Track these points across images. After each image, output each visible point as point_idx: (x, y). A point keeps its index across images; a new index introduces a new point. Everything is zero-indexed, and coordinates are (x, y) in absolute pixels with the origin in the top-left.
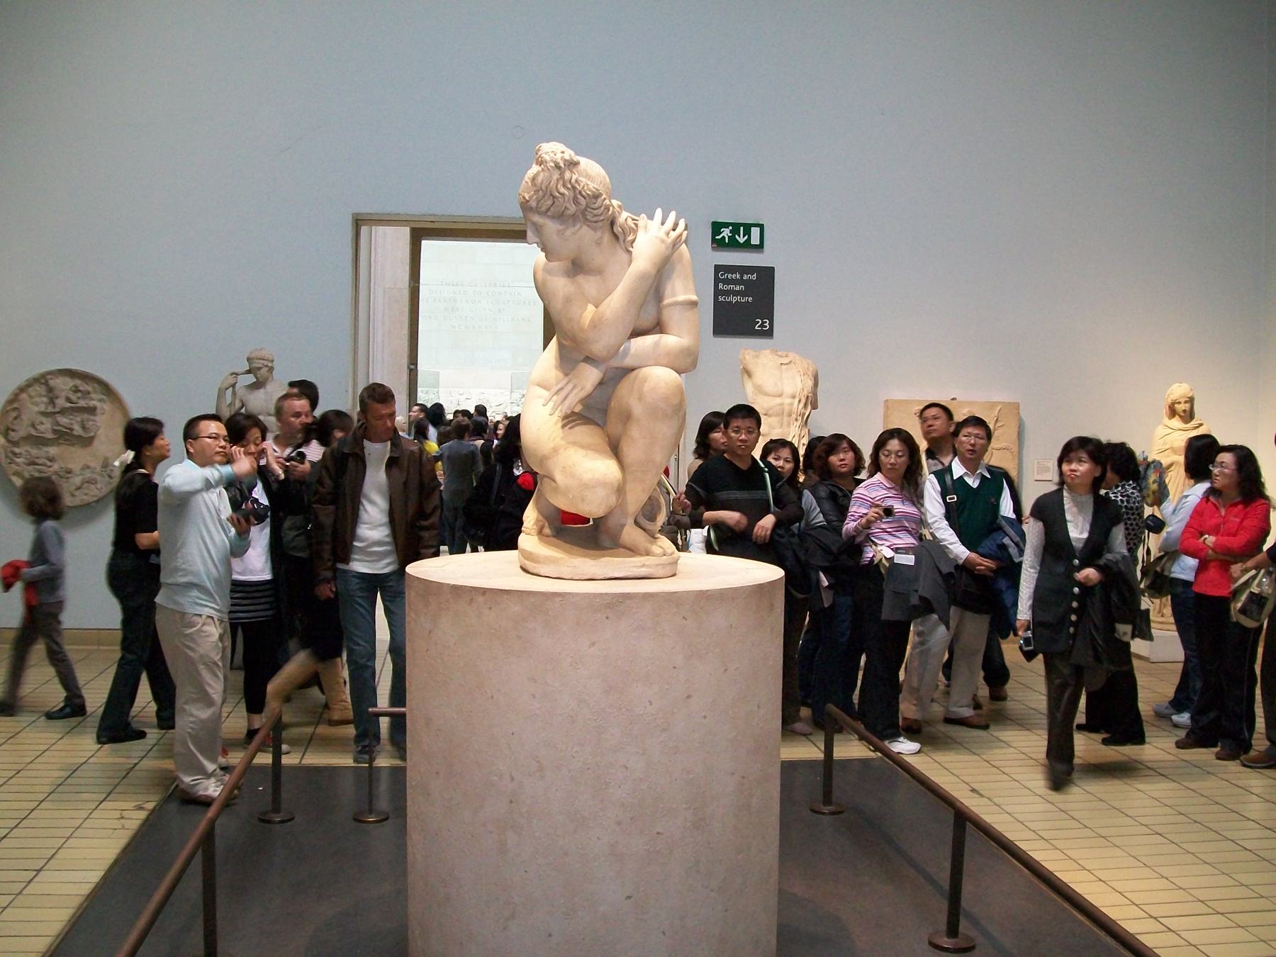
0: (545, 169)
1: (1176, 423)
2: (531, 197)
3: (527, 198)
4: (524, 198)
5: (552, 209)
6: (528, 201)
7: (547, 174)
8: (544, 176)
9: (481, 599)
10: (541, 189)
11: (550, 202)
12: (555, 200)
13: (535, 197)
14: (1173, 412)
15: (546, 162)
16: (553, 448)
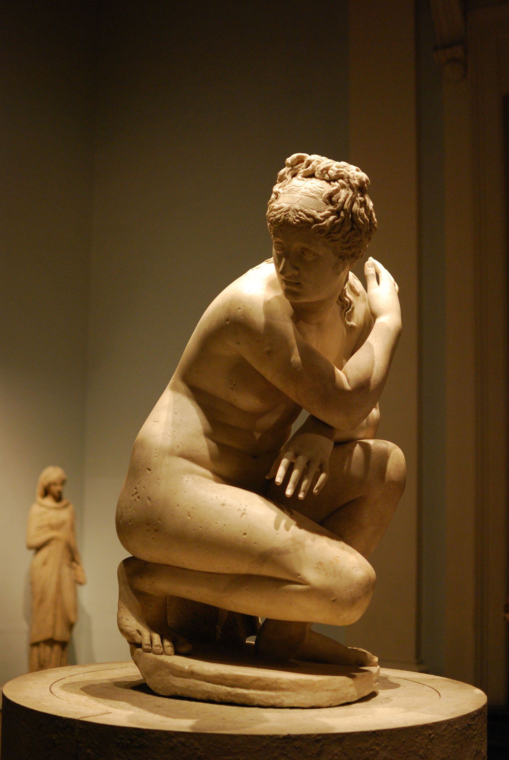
0: (347, 185)
1: (49, 502)
2: (326, 217)
3: (319, 216)
4: (309, 216)
5: (347, 237)
6: (316, 221)
7: (351, 193)
8: (347, 195)
9: (336, 749)
10: (345, 211)
11: (348, 228)
12: (355, 226)
13: (332, 218)
14: (46, 492)
15: (349, 178)
16: (293, 539)
